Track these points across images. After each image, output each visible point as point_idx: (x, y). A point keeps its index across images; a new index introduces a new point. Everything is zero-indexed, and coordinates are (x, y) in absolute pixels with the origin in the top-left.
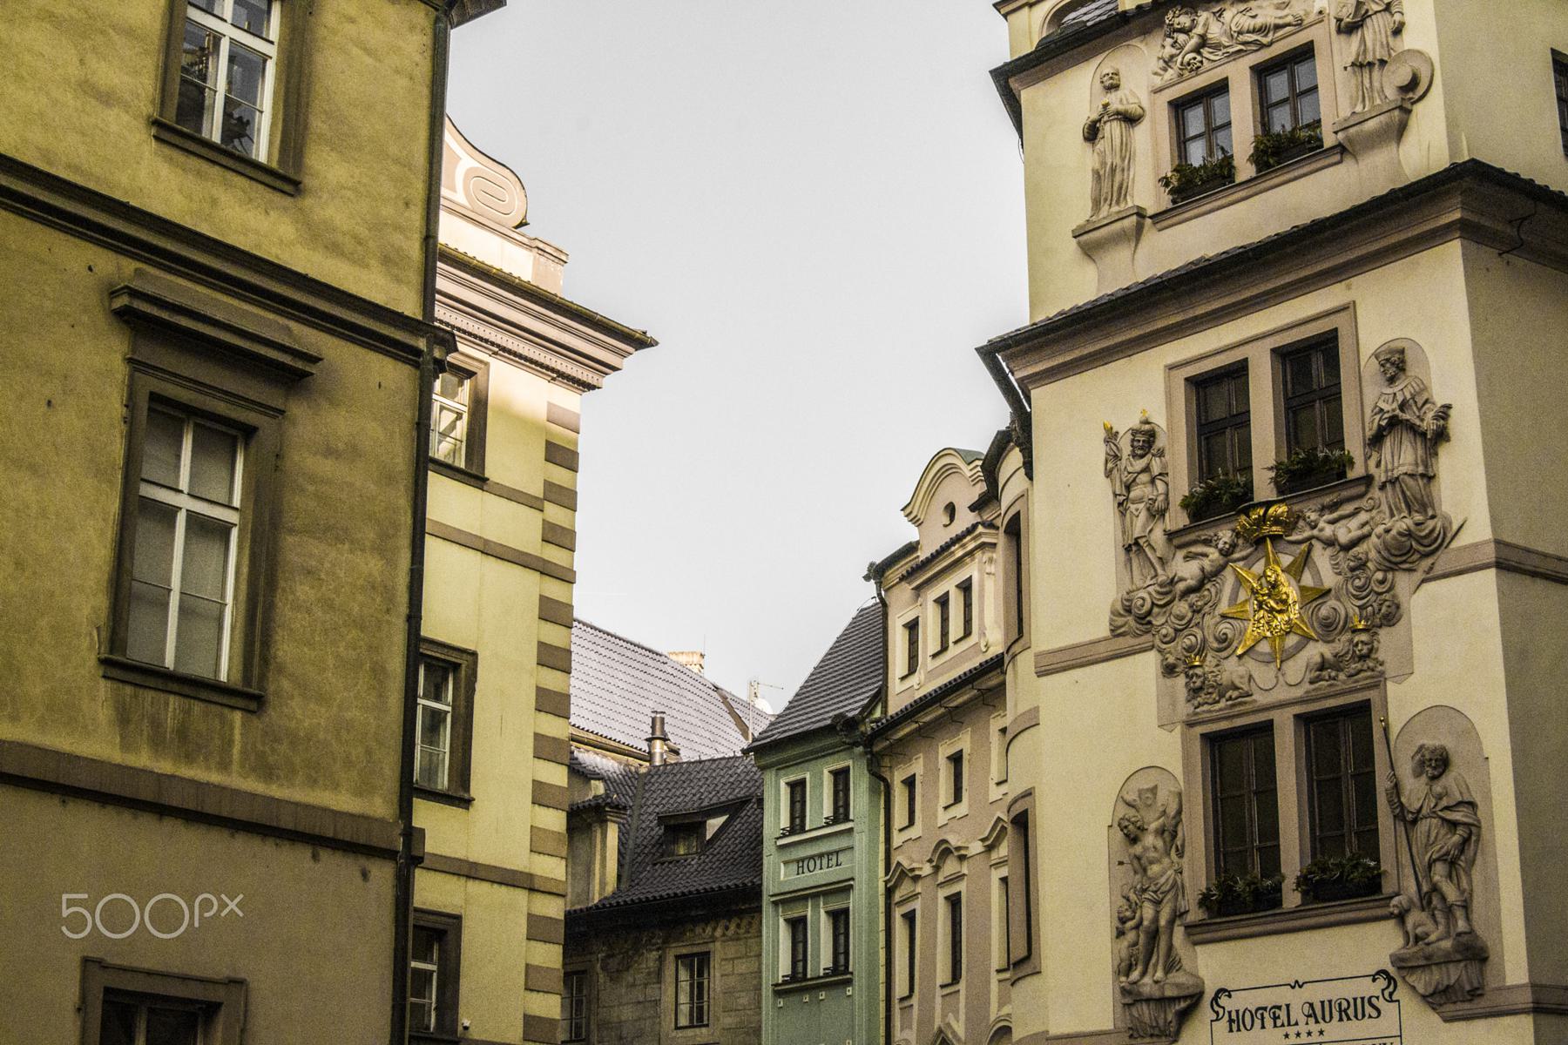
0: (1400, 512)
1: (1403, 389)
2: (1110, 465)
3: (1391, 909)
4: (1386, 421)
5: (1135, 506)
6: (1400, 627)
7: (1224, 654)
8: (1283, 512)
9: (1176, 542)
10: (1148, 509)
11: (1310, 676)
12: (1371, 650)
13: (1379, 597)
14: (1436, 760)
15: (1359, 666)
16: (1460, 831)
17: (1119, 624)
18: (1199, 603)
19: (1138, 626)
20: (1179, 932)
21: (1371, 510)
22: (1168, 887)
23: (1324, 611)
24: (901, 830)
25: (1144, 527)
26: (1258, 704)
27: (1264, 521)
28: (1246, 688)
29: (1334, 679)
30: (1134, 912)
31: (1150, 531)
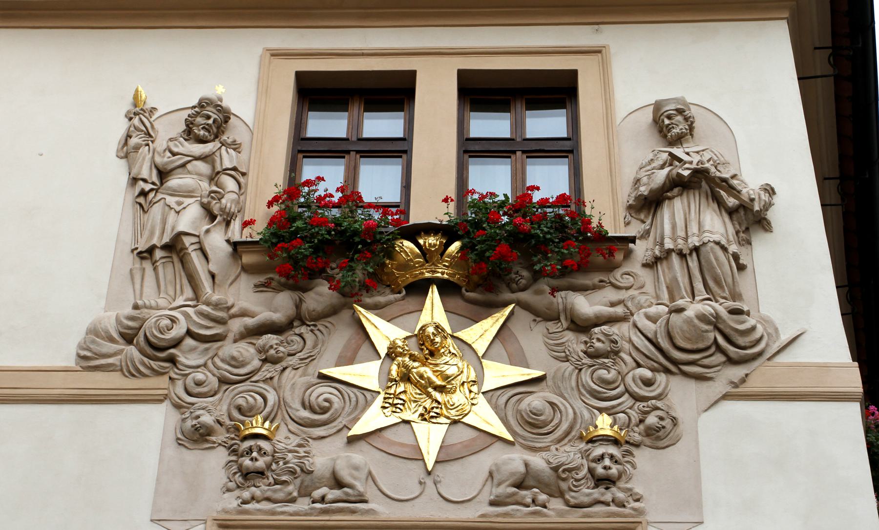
2: (134, 141)
5: (177, 199)
11: (486, 496)
12: (620, 477)
13: (641, 405)
15: (597, 493)
18: (281, 349)
19: (146, 360)
21: (627, 288)
23: (536, 400)
26: (383, 517)
27: (442, 254)
28: (360, 486)
29: (545, 507)
31: (208, 231)
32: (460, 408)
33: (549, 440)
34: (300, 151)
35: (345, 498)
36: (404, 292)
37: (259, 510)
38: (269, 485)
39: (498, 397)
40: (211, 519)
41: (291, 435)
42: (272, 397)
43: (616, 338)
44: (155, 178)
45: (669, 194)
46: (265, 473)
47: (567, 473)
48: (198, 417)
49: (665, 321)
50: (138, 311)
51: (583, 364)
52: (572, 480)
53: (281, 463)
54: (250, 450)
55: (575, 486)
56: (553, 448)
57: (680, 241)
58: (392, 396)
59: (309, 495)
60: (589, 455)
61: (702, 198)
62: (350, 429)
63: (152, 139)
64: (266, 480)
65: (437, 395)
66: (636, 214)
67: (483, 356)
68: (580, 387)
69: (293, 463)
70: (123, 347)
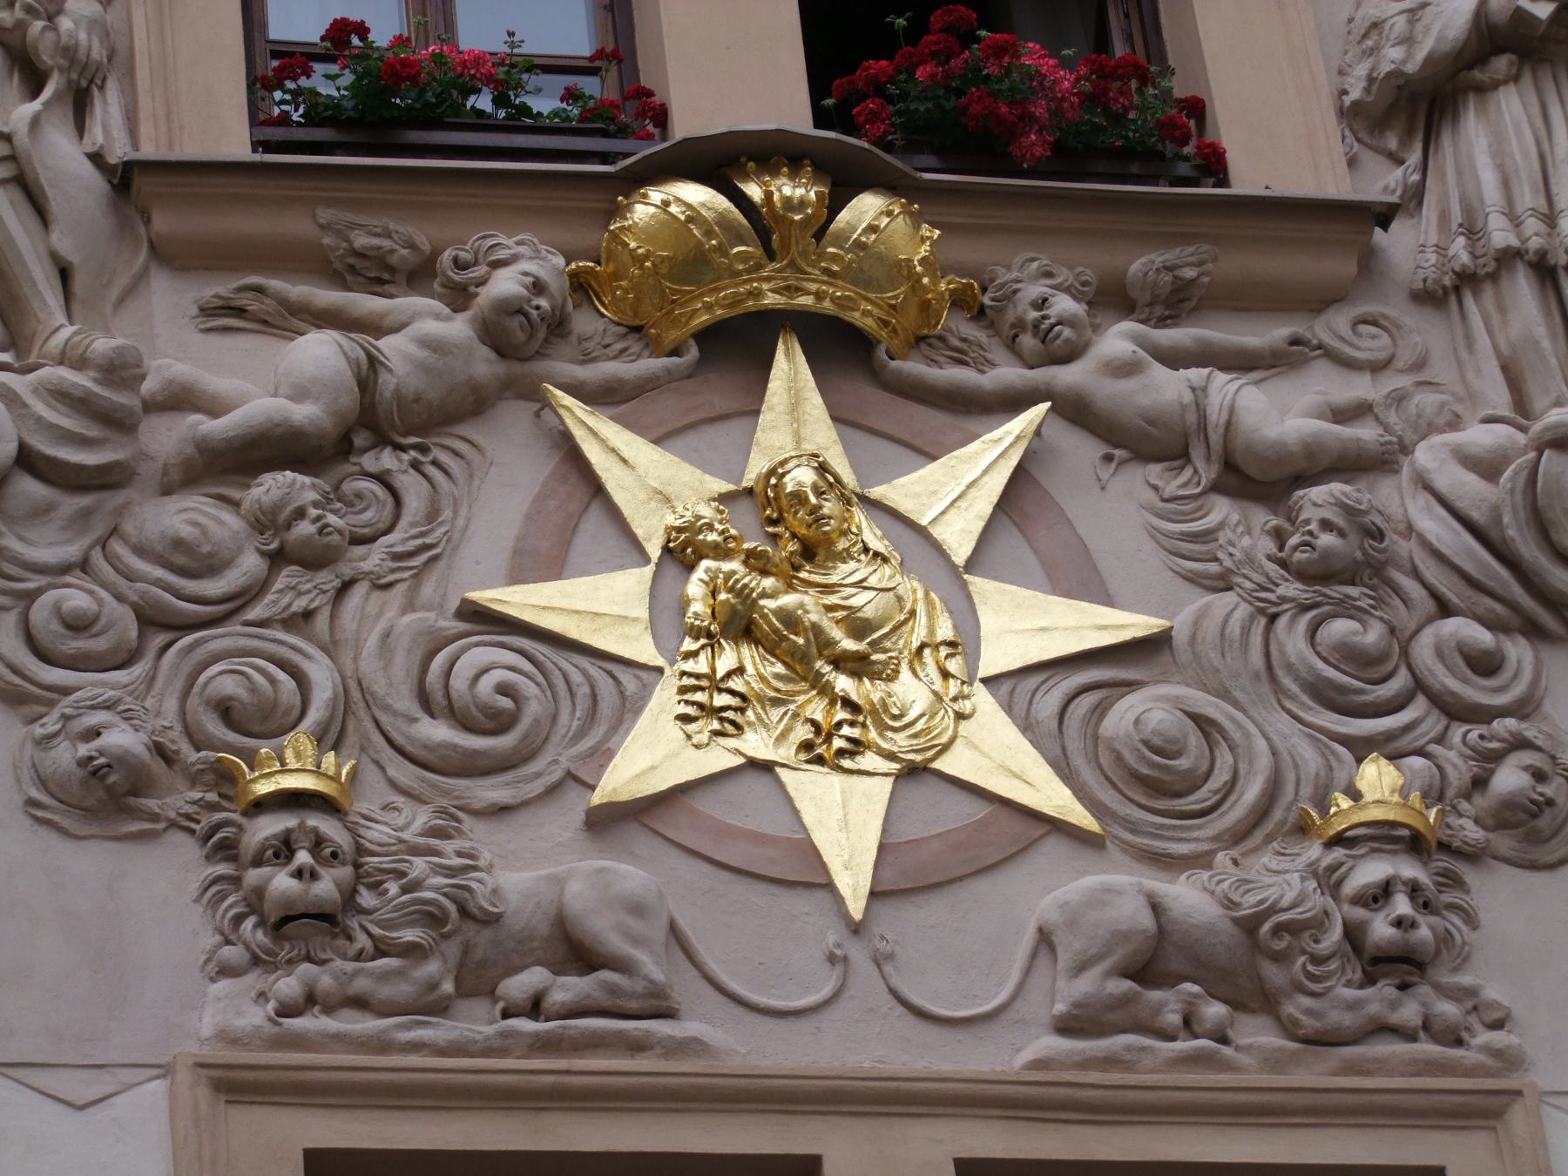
7: (490, 791)
9: (164, 222)
15: (1378, 998)
21: (1378, 368)
26: (732, 1064)
27: (820, 235)
28: (652, 967)
29: (1224, 1040)
32: (920, 726)
33: (1209, 832)
35: (606, 1002)
36: (693, 353)
38: (359, 957)
39: (1034, 694)
40: (191, 1061)
41: (399, 800)
42: (321, 674)
45: (1478, 75)
46: (339, 917)
47: (1288, 937)
48: (94, 733)
49: (1524, 474)
51: (1284, 599)
52: (1302, 959)
53: (393, 888)
54: (283, 849)
55: (1313, 978)
56: (1222, 858)
57: (1532, 225)
58: (705, 683)
59: (492, 994)
60: (1340, 883)
62: (593, 788)
64: (341, 942)
65: (843, 683)
66: (1371, 132)
67: (972, 564)
68: (1280, 672)
69: (437, 889)
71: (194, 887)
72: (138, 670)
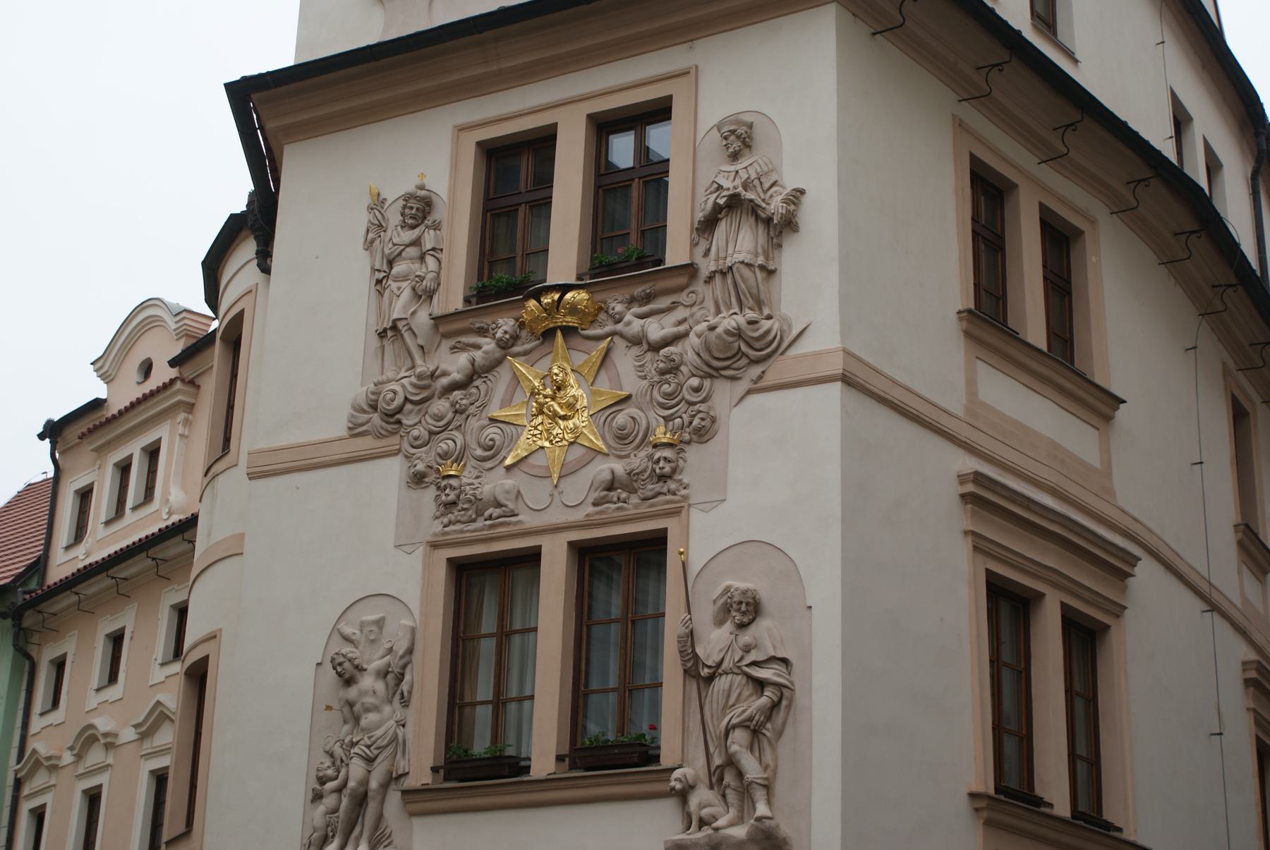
0: (729, 307)
1: (749, 165)
2: (371, 235)
3: (673, 784)
4: (725, 199)
6: (713, 446)
7: (488, 465)
8: (582, 300)
9: (442, 329)
10: (414, 289)
12: (674, 471)
14: (747, 604)
15: (657, 487)
16: (769, 692)
17: (360, 421)
18: (464, 402)
19: (384, 425)
20: (394, 798)
21: (692, 306)
22: (386, 742)
24: (42, 714)
25: (405, 308)
26: (524, 527)
27: (557, 309)
28: (511, 506)
29: (625, 502)
30: (338, 771)
31: (414, 313)
34: (487, 211)
35: (503, 514)
37: (455, 531)
38: (459, 511)
41: (472, 470)
43: (674, 357)
44: (385, 267)
45: (720, 216)
48: (415, 466)
50: (376, 388)
51: (655, 381)
55: (642, 485)
56: (632, 455)
61: (743, 216)
63: (384, 229)
65: (560, 422)
70: (371, 415)
71: (434, 496)
72: (428, 447)
